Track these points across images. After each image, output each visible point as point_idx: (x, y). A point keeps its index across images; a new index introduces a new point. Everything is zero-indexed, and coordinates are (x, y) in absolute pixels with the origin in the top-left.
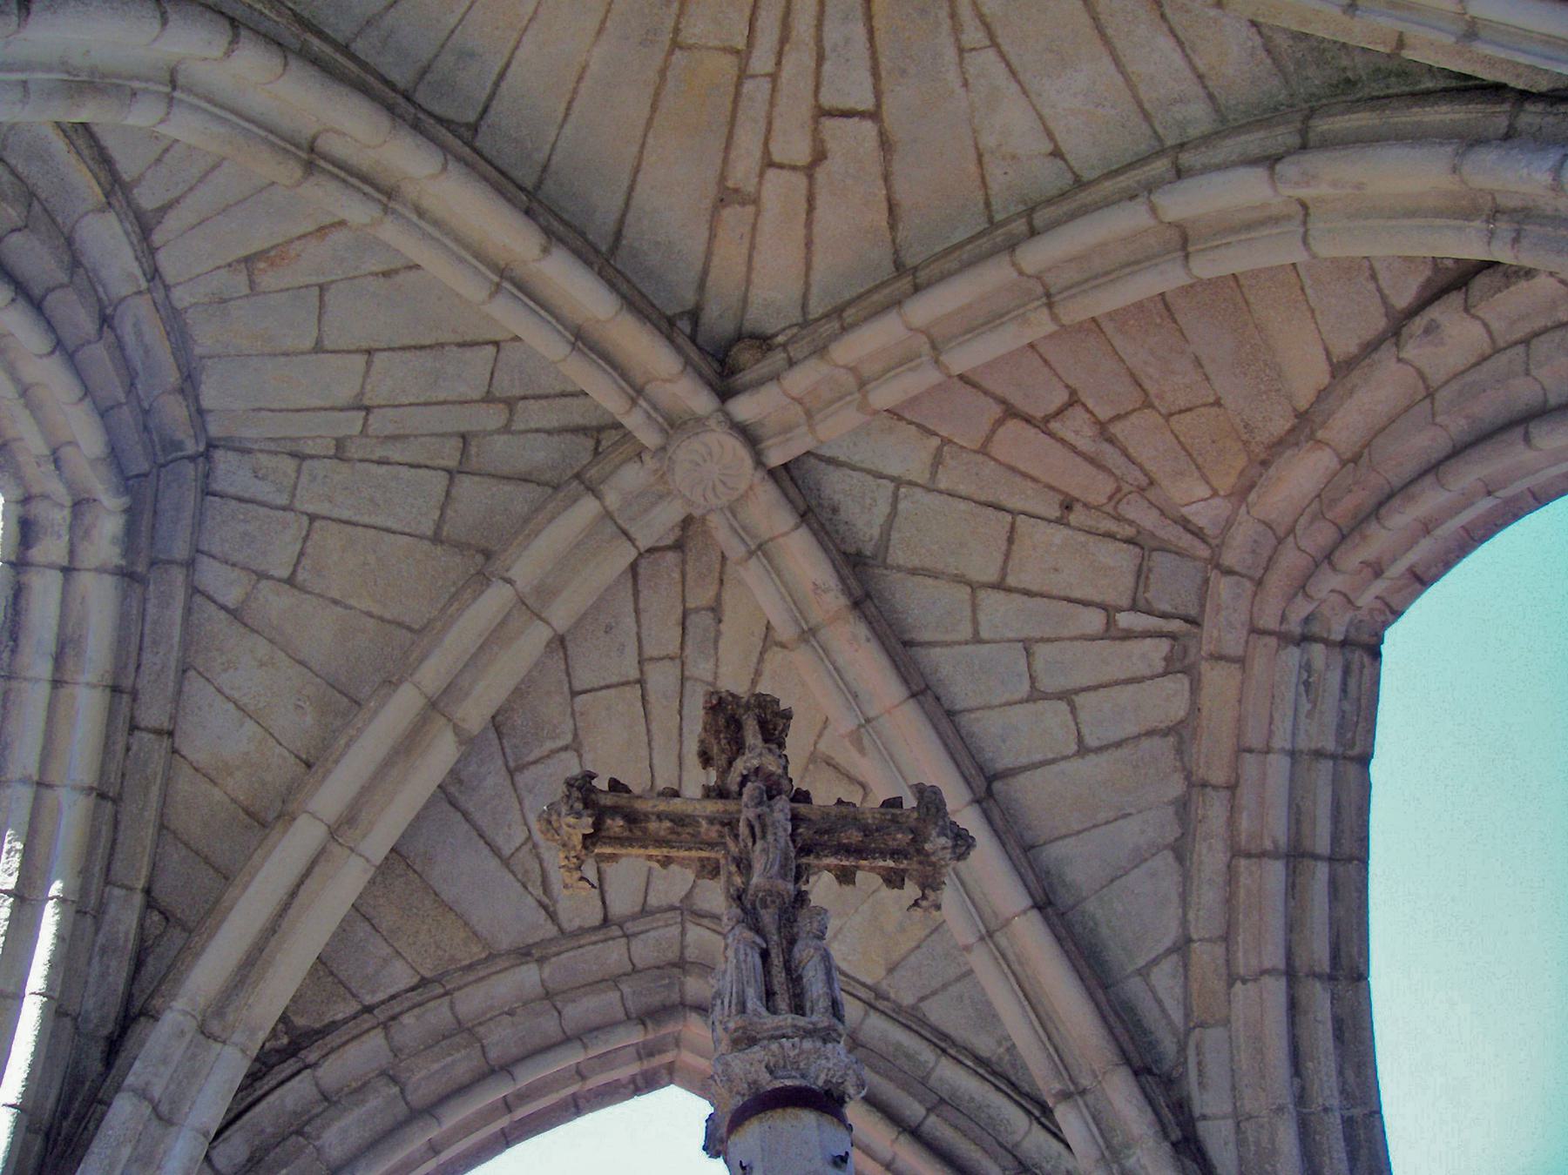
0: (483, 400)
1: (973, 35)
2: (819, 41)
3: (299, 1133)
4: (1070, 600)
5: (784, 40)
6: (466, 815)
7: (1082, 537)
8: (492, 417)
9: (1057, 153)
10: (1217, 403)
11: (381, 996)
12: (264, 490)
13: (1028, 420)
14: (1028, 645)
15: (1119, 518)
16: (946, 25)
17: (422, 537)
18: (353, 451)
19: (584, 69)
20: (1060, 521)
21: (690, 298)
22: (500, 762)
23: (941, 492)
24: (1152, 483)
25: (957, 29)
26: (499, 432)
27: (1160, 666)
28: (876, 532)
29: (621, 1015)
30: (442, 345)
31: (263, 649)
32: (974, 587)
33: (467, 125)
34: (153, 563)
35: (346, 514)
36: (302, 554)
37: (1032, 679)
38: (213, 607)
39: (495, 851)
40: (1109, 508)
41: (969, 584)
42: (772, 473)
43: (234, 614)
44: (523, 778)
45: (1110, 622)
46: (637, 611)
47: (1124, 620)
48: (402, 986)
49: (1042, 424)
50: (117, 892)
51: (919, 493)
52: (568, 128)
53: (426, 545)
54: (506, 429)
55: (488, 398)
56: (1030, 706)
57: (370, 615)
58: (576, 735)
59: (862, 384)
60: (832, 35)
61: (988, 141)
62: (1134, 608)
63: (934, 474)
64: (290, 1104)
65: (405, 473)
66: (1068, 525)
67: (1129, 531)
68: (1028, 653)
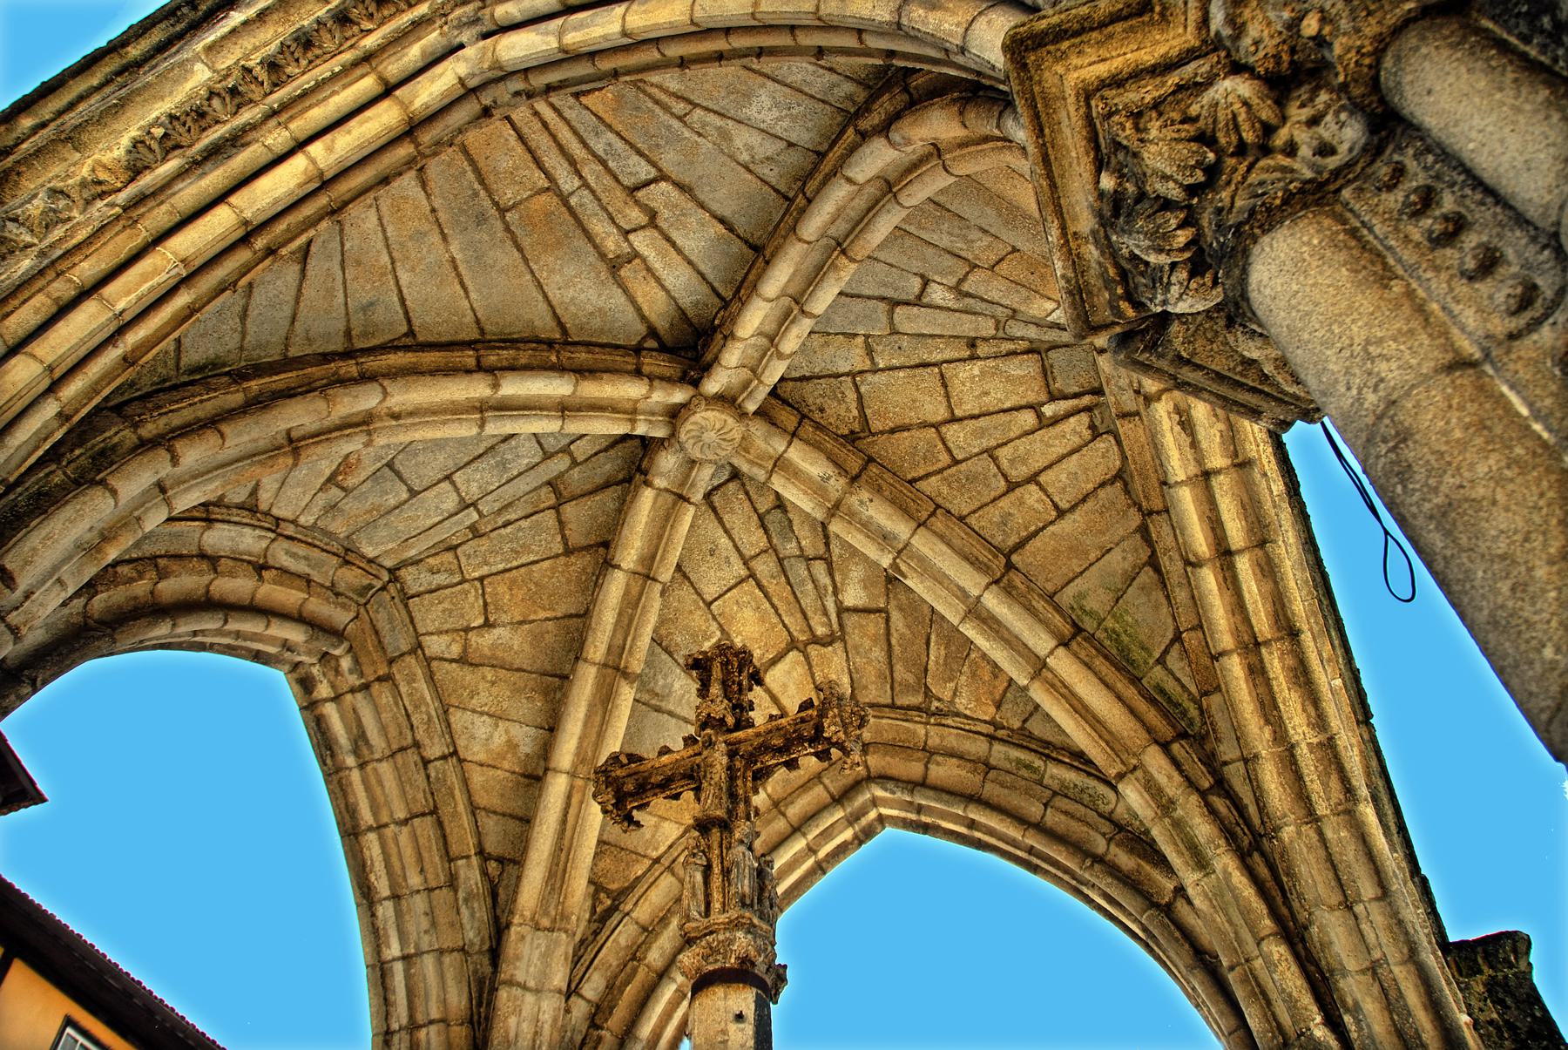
0: (544, 460)
1: (679, 108)
2: (594, 155)
3: (633, 958)
4: (1004, 411)
5: (572, 162)
6: (671, 714)
7: (992, 363)
8: (560, 464)
9: (791, 145)
10: (1015, 250)
11: (662, 849)
12: (441, 579)
13: (907, 303)
14: (990, 452)
15: (1012, 339)
16: (657, 109)
17: (557, 556)
18: (483, 529)
19: (453, 260)
20: (973, 358)
21: (642, 329)
23: (882, 370)
24: (1014, 311)
25: (666, 108)
26: (570, 468)
27: (1087, 434)
28: (855, 413)
29: (829, 800)
30: (492, 447)
31: (489, 674)
32: (936, 426)
33: (406, 335)
34: (391, 662)
35: (501, 567)
36: (486, 604)
37: (1005, 476)
38: (446, 664)
40: (1001, 334)
41: (932, 426)
42: (761, 413)
43: (462, 660)
45: (1040, 416)
46: (726, 531)
47: (1048, 410)
48: (674, 837)
49: (918, 301)
50: (460, 862)
51: (870, 377)
52: (473, 296)
53: (562, 560)
54: (575, 463)
55: (548, 456)
56: (1012, 496)
58: (723, 630)
59: (772, 340)
60: (599, 148)
61: (745, 157)
62: (1053, 398)
63: (872, 359)
64: (623, 941)
65: (524, 524)
66: (979, 358)
67: (1024, 345)
68: (995, 459)
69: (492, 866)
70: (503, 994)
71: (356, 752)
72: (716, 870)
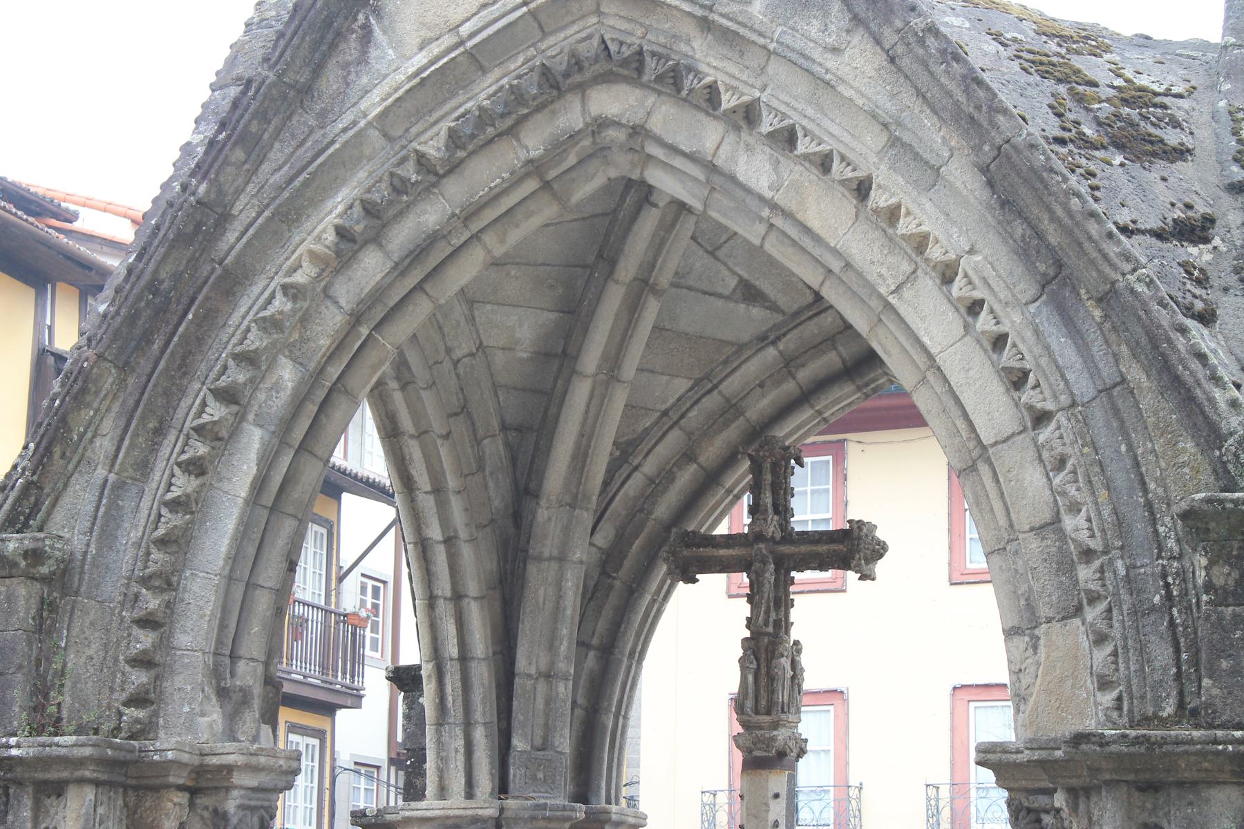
3: (641, 510)
6: (690, 288)
11: (671, 401)
39: (720, 296)
44: (721, 254)
48: (682, 391)
57: (576, 220)
64: (631, 493)
70: (532, 569)
71: (398, 378)
72: (763, 671)
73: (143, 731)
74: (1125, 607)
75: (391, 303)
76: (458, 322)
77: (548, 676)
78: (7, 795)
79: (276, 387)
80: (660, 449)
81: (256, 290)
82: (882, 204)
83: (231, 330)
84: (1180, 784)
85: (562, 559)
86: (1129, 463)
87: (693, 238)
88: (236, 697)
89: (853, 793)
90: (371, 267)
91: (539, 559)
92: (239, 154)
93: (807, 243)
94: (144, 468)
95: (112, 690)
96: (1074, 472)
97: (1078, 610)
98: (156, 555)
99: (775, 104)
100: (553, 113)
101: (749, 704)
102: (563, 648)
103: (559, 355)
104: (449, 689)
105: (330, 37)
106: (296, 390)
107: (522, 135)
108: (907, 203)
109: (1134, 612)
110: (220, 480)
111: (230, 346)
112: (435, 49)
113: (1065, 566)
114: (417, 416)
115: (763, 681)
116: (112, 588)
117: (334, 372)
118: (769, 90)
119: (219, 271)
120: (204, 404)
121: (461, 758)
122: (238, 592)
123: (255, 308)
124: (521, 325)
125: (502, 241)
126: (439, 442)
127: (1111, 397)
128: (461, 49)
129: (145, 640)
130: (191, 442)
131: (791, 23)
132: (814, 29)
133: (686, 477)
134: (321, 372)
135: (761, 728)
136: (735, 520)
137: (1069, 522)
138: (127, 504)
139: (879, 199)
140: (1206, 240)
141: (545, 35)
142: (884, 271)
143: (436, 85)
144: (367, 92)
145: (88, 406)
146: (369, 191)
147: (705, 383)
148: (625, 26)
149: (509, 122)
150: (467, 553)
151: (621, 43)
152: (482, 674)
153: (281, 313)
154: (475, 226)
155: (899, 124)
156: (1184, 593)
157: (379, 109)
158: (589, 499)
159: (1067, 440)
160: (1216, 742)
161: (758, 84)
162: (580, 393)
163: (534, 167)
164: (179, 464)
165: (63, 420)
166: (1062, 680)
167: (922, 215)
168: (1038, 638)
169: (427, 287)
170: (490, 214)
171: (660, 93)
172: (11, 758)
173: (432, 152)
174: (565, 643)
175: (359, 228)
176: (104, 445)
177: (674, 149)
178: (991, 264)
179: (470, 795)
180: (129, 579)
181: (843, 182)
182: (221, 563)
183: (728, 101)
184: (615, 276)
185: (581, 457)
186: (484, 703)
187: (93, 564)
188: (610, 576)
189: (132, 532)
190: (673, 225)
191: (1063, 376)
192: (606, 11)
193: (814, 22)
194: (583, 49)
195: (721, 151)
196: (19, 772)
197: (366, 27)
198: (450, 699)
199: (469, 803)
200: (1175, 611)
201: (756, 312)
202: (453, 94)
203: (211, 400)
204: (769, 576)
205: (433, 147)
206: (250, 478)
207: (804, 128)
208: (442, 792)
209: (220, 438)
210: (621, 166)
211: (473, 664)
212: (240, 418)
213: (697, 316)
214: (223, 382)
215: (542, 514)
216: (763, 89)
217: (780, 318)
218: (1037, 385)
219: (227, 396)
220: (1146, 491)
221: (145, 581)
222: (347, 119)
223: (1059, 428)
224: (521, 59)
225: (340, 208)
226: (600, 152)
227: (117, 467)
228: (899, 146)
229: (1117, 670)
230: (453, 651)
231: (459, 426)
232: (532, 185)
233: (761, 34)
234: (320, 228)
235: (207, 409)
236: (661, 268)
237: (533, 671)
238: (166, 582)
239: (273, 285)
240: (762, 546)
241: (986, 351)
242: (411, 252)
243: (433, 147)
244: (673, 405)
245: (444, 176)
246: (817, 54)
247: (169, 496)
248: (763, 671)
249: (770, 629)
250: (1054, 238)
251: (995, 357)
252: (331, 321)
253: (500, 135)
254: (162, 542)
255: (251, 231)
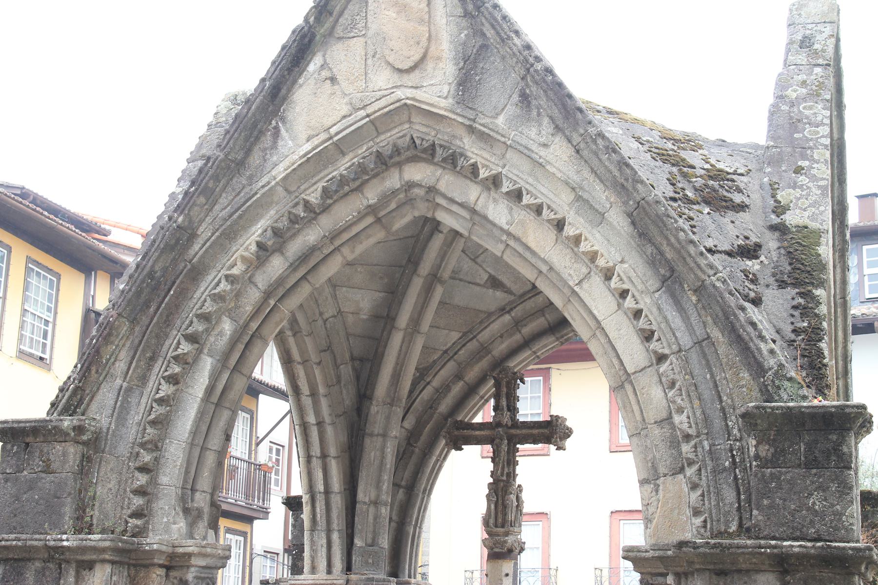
3: (431, 408)
6: (461, 280)
11: (449, 345)
22: (467, 259)
44: (479, 260)
64: (426, 398)
69: (357, 363)
70: (367, 441)
71: (291, 329)
72: (500, 502)
73: (140, 532)
74: (709, 468)
75: (288, 286)
76: (327, 298)
77: (376, 503)
78: (60, 568)
79: (221, 334)
80: (442, 372)
81: (210, 278)
82: (571, 234)
83: (195, 301)
84: (739, 571)
85: (384, 435)
86: (711, 385)
87: (463, 251)
88: (194, 513)
89: (553, 572)
90: (277, 265)
91: (371, 435)
92: (202, 200)
93: (528, 255)
94: (144, 379)
95: (122, 508)
96: (680, 390)
97: (682, 470)
98: (149, 430)
99: (511, 175)
100: (383, 178)
101: (492, 521)
102: (385, 487)
103: (385, 317)
104: (318, 510)
105: (256, 133)
106: (232, 337)
107: (365, 191)
108: (586, 234)
109: (714, 471)
110: (187, 387)
111: (194, 310)
112: (316, 141)
113: (674, 444)
114: (303, 351)
115: (500, 508)
116: (123, 449)
117: (254, 325)
118: (507, 168)
119: (189, 266)
120: (179, 343)
121: (324, 550)
122: (196, 452)
123: (210, 288)
124: (363, 300)
125: (353, 252)
126: (315, 366)
127: (701, 347)
128: (331, 141)
129: (142, 479)
130: (171, 365)
131: (520, 129)
132: (533, 133)
133: (457, 389)
134: (246, 325)
135: (498, 535)
136: (484, 415)
137: (677, 419)
138: (133, 400)
139: (569, 231)
140: (757, 257)
141: (379, 134)
142: (572, 272)
143: (316, 161)
144: (276, 165)
145: (112, 343)
146: (276, 222)
147: (468, 335)
148: (424, 129)
149: (358, 183)
150: (329, 431)
151: (423, 139)
152: (338, 502)
153: (224, 291)
154: (337, 243)
155: (581, 188)
156: (743, 460)
157: (283, 175)
158: (401, 400)
159: (676, 371)
160: (760, 547)
161: (501, 164)
162: (397, 339)
163: (372, 210)
164: (164, 378)
165: (98, 352)
166: (672, 510)
167: (594, 241)
168: (659, 486)
169: (309, 277)
170: (346, 236)
171: (444, 168)
172: (63, 547)
173: (313, 200)
174: (386, 484)
175: (270, 243)
176: (120, 367)
177: (452, 201)
178: (633, 269)
179: (329, 572)
180: (133, 443)
181: (549, 221)
182: (187, 435)
183: (483, 174)
184: (418, 272)
185: (396, 377)
186: (338, 518)
187: (113, 435)
188: (412, 446)
189: (136, 416)
190: (451, 243)
191: (674, 334)
192: (414, 121)
193: (533, 129)
194: (400, 143)
195: (479, 202)
196: (67, 555)
197: (277, 128)
198: (319, 516)
199: (329, 577)
200: (737, 470)
201: (499, 294)
202: (326, 167)
203: (183, 341)
204: (504, 447)
205: (314, 197)
206: (204, 387)
207: (527, 190)
208: (313, 570)
209: (188, 363)
210: (421, 209)
211: (332, 496)
212: (200, 351)
213: (463, 296)
214: (190, 331)
215: (374, 409)
216: (504, 166)
217: (512, 298)
218: (659, 339)
219: (192, 339)
220: (721, 401)
221: (143, 445)
222: (264, 180)
223: (671, 364)
224: (365, 148)
225: (260, 231)
226: (410, 202)
227: (128, 379)
228: (581, 201)
229: (704, 504)
230: (321, 488)
231: (327, 357)
232: (370, 220)
233: (503, 136)
234: (248, 242)
235: (181, 346)
236: (444, 268)
237: (367, 500)
238: (155, 446)
239: (220, 275)
240: (500, 429)
241: (630, 319)
242: (300, 257)
243: (314, 197)
244: (451, 347)
245: (319, 214)
246: (534, 147)
247: (158, 396)
248: (500, 502)
249: (504, 478)
250: (669, 254)
251: (635, 322)
252: (253, 296)
253: (352, 191)
254: (153, 423)
255: (208, 244)
